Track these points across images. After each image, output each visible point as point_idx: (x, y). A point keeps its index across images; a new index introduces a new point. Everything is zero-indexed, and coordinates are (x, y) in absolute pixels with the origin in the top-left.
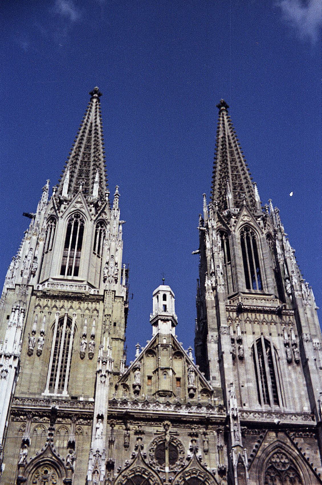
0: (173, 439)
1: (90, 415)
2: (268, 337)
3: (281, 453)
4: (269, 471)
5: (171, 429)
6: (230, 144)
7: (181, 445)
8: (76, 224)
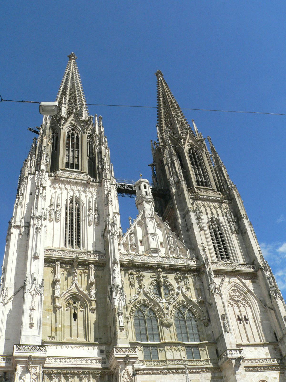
0: (165, 281)
1: (103, 264)
2: (216, 217)
3: (235, 290)
4: (230, 301)
5: (162, 274)
6: (169, 96)
7: (171, 285)
8: (73, 134)
